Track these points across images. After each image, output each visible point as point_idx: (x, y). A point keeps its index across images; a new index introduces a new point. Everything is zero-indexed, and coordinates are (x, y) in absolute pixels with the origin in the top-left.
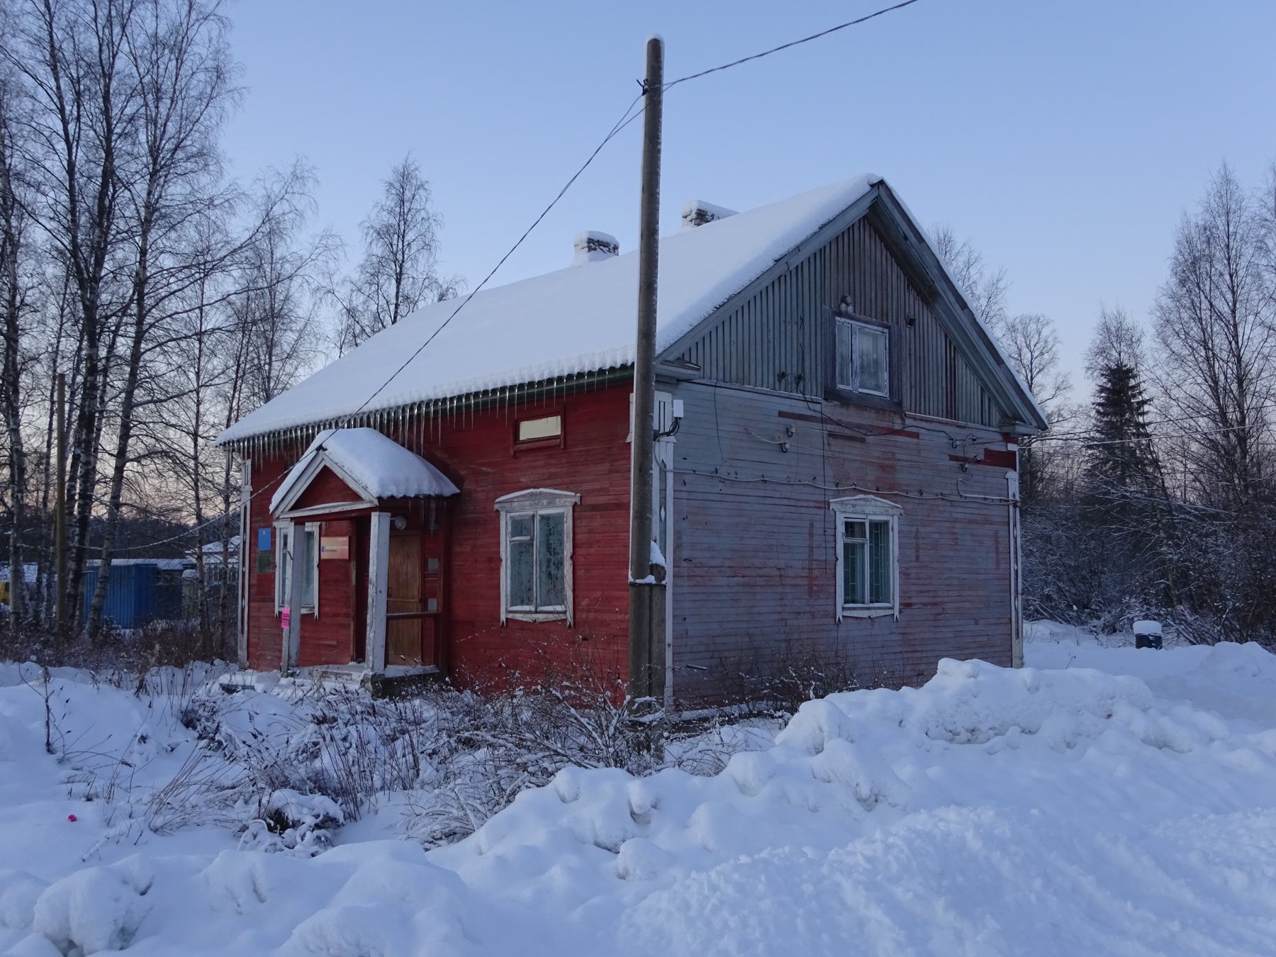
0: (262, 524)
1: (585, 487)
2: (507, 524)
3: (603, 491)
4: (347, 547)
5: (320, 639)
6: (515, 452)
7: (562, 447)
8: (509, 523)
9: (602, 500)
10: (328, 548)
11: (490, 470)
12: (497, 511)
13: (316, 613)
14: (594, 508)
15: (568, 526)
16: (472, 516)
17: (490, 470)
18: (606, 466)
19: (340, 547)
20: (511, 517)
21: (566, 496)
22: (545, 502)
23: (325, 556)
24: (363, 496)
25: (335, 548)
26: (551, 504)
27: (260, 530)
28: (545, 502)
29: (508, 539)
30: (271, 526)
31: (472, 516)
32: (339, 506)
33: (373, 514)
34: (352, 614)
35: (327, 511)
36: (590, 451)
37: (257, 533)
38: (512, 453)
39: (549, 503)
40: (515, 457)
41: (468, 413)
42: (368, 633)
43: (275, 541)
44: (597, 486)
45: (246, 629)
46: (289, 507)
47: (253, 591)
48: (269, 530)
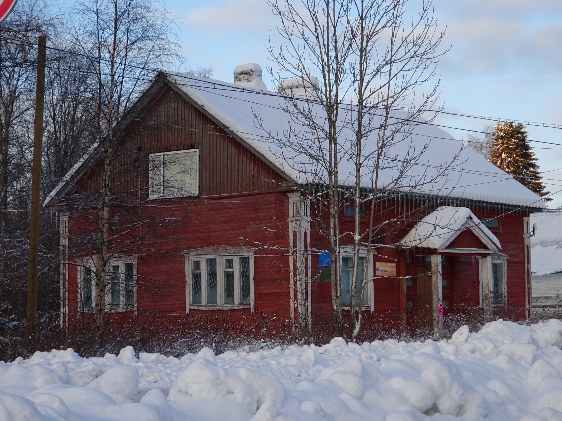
4: (395, 270)
7: (501, 233)
10: (381, 269)
13: (372, 310)
15: (505, 270)
19: (390, 269)
21: (504, 256)
22: (496, 257)
24: (489, 247)
25: (386, 269)
26: (499, 259)
28: (496, 257)
32: (475, 250)
35: (469, 252)
39: (498, 258)
41: (483, 209)
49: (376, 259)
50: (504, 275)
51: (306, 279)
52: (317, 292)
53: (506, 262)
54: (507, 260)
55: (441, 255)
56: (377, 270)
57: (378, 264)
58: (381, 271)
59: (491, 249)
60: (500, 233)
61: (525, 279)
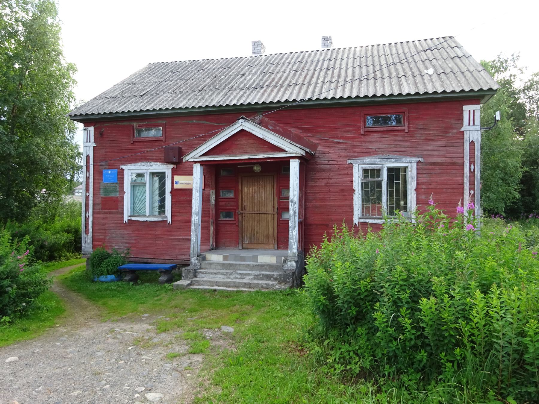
0: (107, 167)
1: (425, 153)
2: (358, 171)
3: (439, 156)
5: (173, 235)
6: (365, 132)
7: (407, 131)
8: (361, 171)
9: (439, 160)
11: (341, 141)
12: (351, 164)
13: (169, 220)
14: (434, 164)
16: (322, 166)
17: (341, 141)
18: (443, 142)
20: (362, 167)
23: (176, 186)
24: (287, 149)
27: (105, 172)
29: (360, 179)
30: (118, 168)
31: (322, 166)
33: (291, 160)
34: (211, 220)
36: (430, 134)
37: (101, 173)
38: (363, 133)
40: (363, 135)
42: (290, 232)
43: (123, 179)
44: (436, 153)
45: (91, 230)
46: (201, 154)
47: (98, 207)
48: (115, 171)
49: (174, 172)
50: (410, 180)
51: (87, 194)
52: (100, 205)
53: (415, 165)
54: (418, 162)
55: (199, 165)
56: (176, 183)
57: (176, 178)
58: (181, 184)
59: (292, 151)
60: (404, 130)
61: (463, 184)
